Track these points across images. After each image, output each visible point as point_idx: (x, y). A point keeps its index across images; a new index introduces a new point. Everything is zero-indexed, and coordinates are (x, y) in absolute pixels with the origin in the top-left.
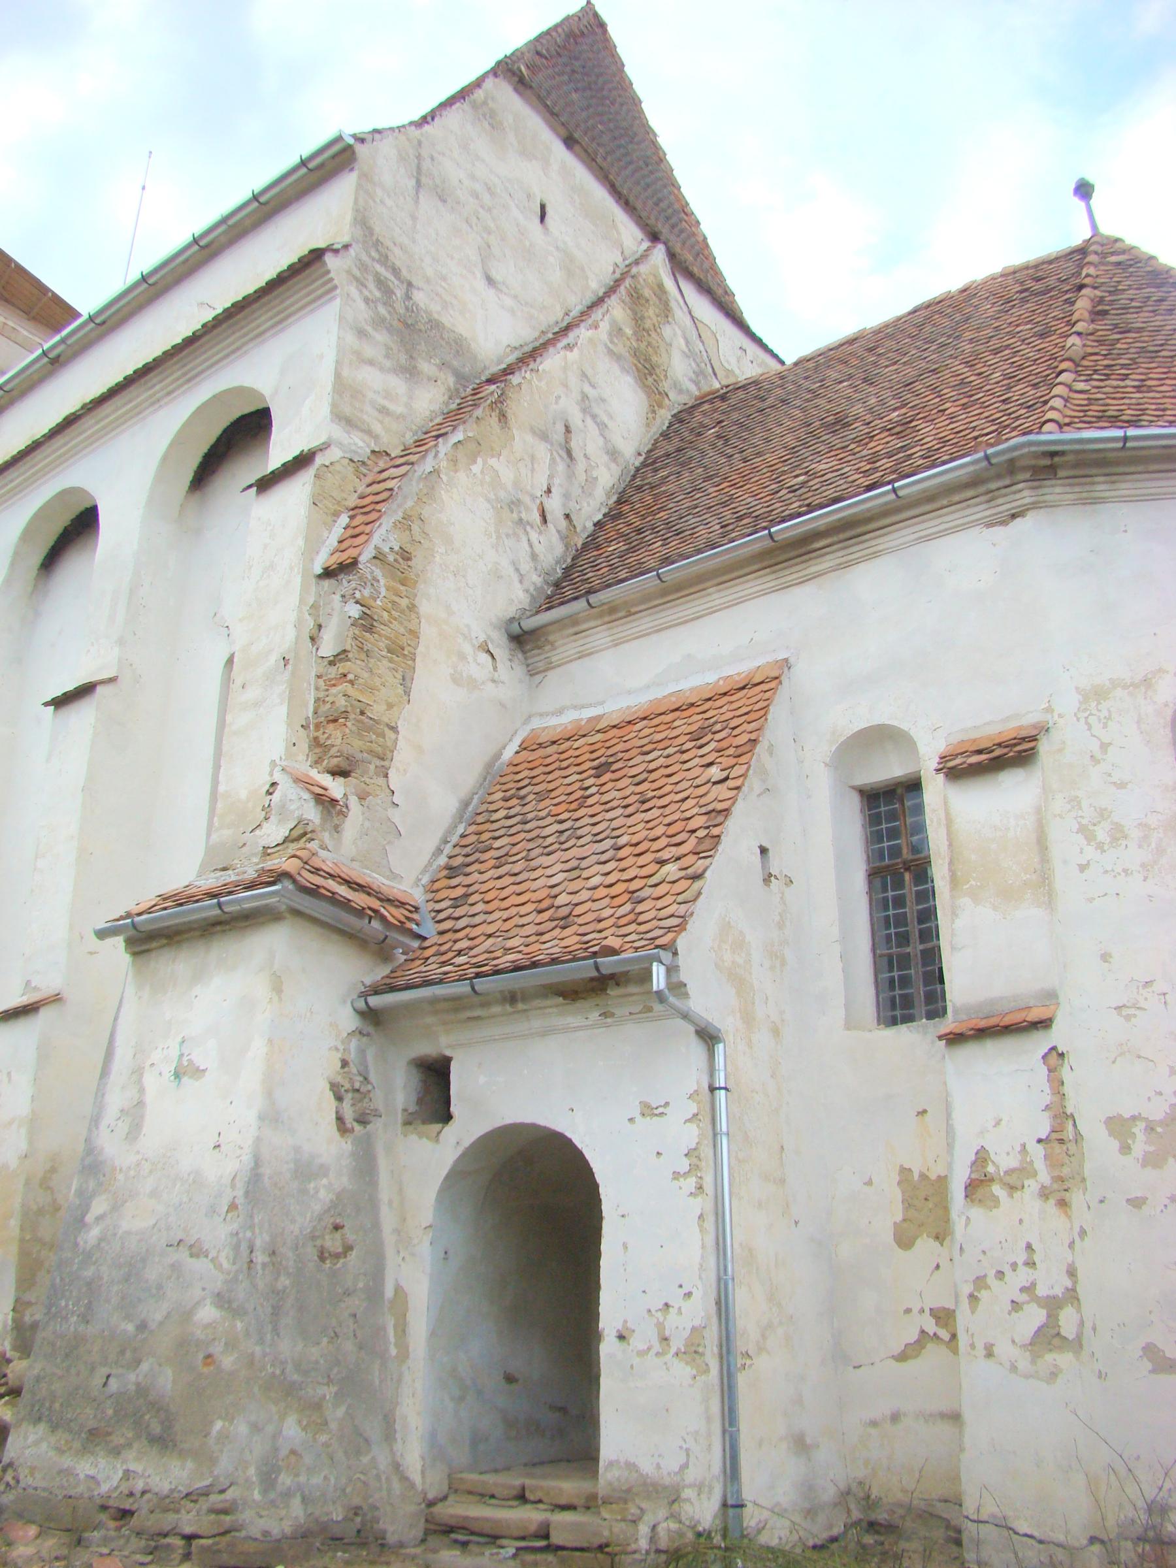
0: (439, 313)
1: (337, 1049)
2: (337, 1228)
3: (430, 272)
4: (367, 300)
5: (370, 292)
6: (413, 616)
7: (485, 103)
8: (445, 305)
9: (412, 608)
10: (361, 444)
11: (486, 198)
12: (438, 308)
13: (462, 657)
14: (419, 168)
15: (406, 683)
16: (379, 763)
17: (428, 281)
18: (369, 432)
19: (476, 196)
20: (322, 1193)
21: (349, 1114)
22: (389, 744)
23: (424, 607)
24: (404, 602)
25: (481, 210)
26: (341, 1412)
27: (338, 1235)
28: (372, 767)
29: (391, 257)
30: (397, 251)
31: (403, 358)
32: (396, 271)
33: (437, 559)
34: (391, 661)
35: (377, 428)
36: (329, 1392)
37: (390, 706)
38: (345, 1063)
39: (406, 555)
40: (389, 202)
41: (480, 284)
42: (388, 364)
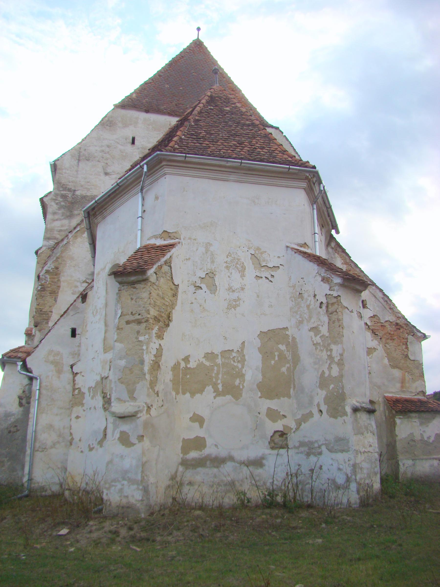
0: (86, 193)
1: (22, 389)
2: (16, 426)
3: (83, 183)
4: (57, 204)
5: (59, 200)
6: (59, 282)
7: (108, 121)
8: (88, 190)
9: (59, 280)
10: (52, 243)
11: (107, 150)
12: (86, 192)
13: (76, 287)
14: (79, 156)
15: (56, 300)
16: (46, 321)
17: (82, 186)
18: (55, 238)
19: (103, 151)
20: (12, 419)
21: (24, 401)
22: (50, 315)
23: (62, 279)
24: (56, 280)
25: (104, 155)
26: (9, 463)
27: (15, 428)
28: (44, 323)
29: (68, 187)
30: (70, 184)
31: (68, 214)
32: (69, 190)
33: (68, 265)
34: (51, 296)
35: (58, 236)
36: (6, 460)
37: (50, 307)
38: (24, 392)
39: (57, 268)
40: (67, 172)
41: (103, 177)
42: (63, 217)
